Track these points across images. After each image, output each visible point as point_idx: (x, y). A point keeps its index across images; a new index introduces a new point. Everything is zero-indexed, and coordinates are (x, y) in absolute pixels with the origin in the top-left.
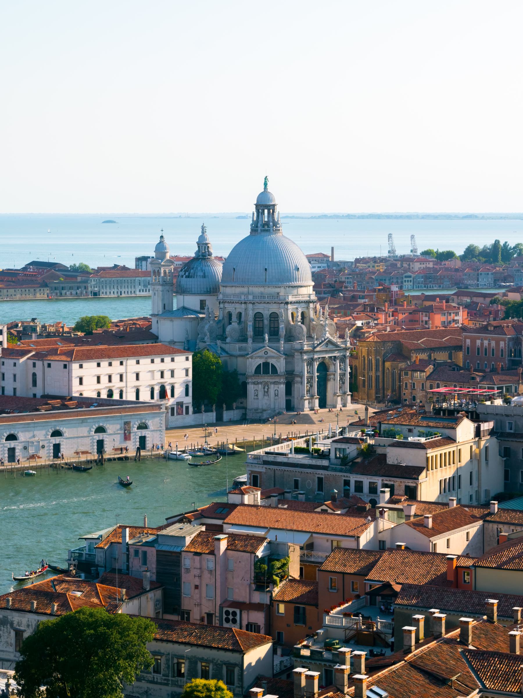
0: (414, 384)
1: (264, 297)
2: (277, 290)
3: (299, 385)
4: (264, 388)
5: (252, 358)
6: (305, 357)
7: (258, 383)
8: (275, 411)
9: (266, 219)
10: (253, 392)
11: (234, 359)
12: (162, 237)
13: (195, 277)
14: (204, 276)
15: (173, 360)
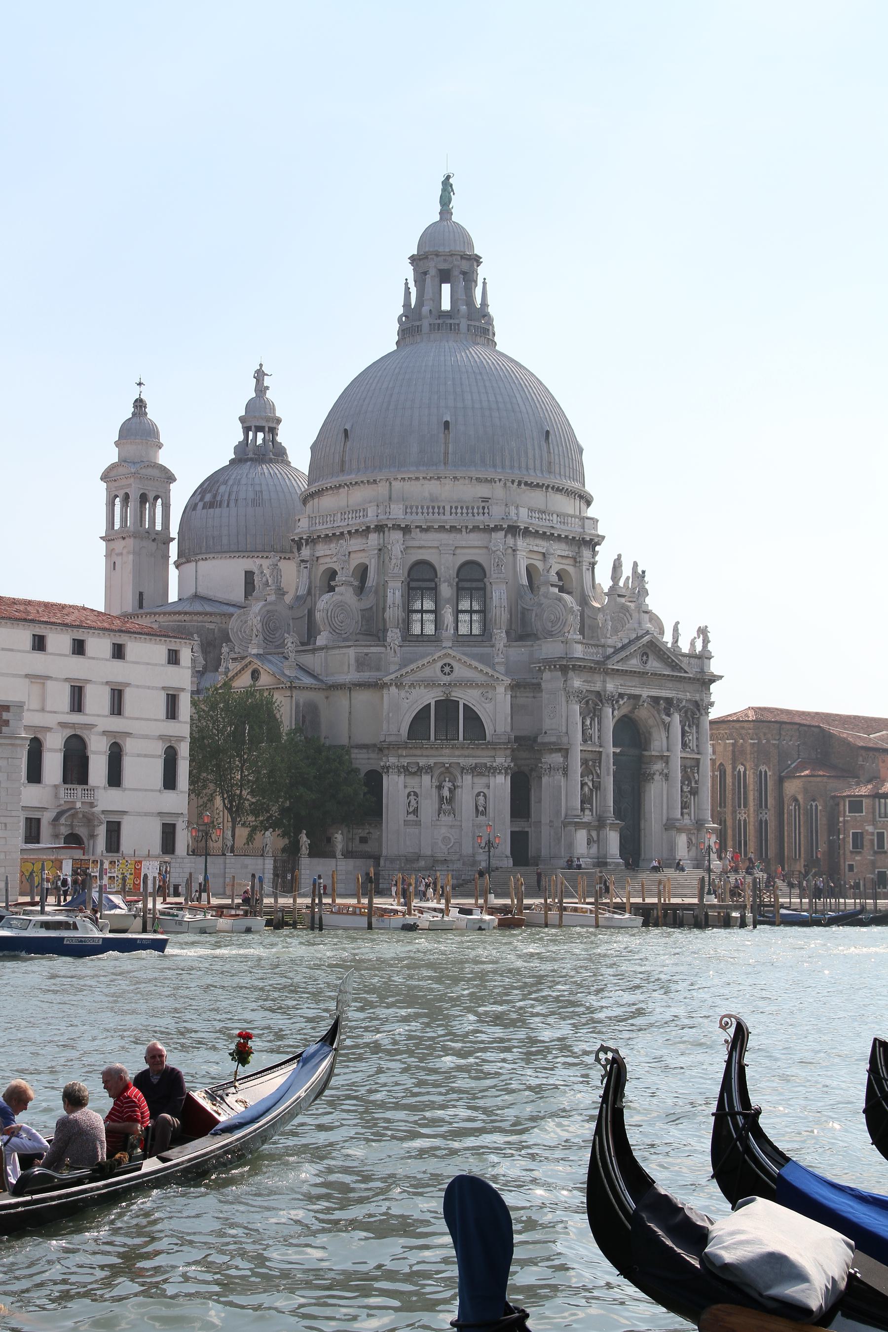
0: (881, 836)
1: (442, 510)
2: (483, 490)
3: (559, 777)
4: (440, 787)
5: (399, 686)
6: (577, 683)
7: (419, 771)
8: (474, 863)
9: (446, 288)
10: (403, 800)
11: (342, 700)
12: (140, 405)
13: (232, 504)
14: (257, 502)
15: (119, 652)
